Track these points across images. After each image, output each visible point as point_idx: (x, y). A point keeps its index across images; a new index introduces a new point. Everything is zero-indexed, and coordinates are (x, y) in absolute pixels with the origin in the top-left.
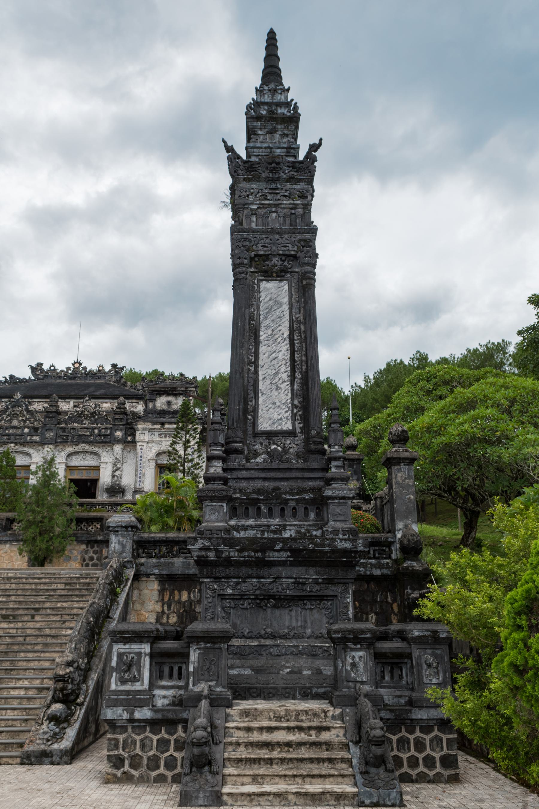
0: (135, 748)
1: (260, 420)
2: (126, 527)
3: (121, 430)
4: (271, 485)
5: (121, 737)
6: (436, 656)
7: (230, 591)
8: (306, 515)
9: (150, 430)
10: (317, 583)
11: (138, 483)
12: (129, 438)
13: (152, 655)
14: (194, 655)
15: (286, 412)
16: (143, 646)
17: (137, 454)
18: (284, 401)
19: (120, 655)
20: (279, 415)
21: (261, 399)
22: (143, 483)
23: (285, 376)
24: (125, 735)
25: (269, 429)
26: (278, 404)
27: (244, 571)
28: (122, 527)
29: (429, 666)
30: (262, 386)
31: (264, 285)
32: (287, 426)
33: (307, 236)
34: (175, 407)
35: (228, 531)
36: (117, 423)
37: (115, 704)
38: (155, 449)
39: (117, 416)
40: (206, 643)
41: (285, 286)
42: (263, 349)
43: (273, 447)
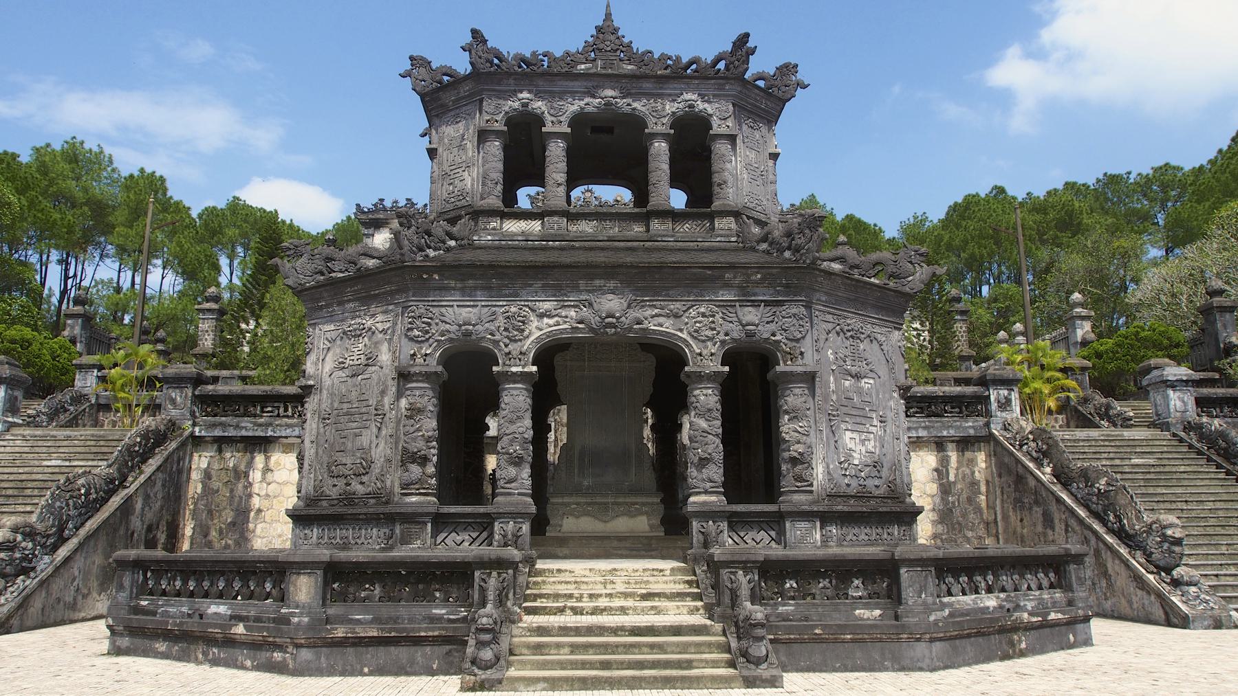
2: (1187, 382)
28: (1183, 381)
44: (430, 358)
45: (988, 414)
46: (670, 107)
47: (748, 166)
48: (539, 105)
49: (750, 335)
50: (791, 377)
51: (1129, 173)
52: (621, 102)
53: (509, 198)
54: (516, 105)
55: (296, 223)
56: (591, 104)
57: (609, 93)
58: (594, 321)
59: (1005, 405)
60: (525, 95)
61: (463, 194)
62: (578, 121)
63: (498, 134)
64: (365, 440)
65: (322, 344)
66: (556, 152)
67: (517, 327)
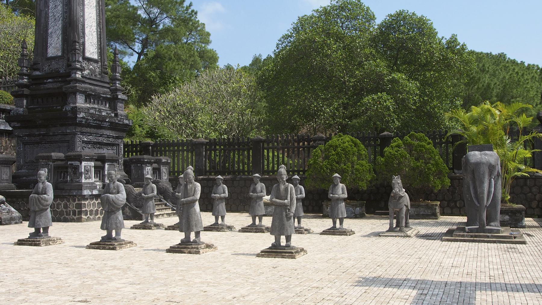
0: (91, 207)
1: (86, 51)
5: (86, 202)
6: (165, 168)
7: (86, 139)
8: (106, 105)
10: (113, 138)
13: (95, 167)
14: (107, 166)
15: (95, 49)
16: (91, 163)
18: (94, 43)
19: (85, 166)
20: (93, 50)
21: (86, 38)
24: (88, 202)
25: (89, 56)
26: (92, 44)
27: (93, 130)
29: (164, 172)
32: (95, 57)
35: (89, 109)
37: (87, 188)
40: (110, 162)
42: (86, 10)
43: (91, 67)
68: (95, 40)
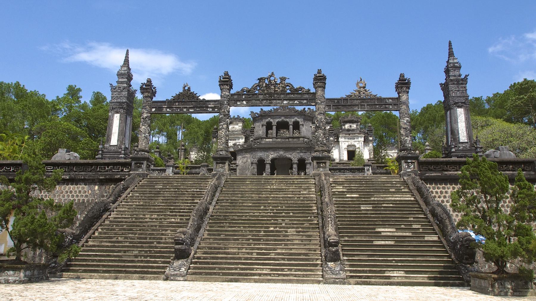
1: (460, 140)
3: (332, 137)
4: (464, 153)
9: (344, 137)
11: (341, 157)
12: (336, 140)
17: (340, 146)
21: (460, 135)
22: (343, 157)
23: (465, 130)
30: (460, 132)
31: (457, 109)
32: (466, 141)
33: (467, 98)
34: (353, 128)
36: (330, 134)
38: (347, 144)
39: (331, 132)
41: (462, 109)
44: (256, 161)
45: (365, 172)
46: (293, 120)
47: (306, 129)
48: (271, 120)
49: (302, 157)
50: (307, 163)
51: (482, 97)
52: (285, 119)
53: (267, 133)
54: (268, 120)
55: (197, 118)
56: (280, 120)
57: (283, 118)
58: (279, 155)
59: (368, 170)
60: (269, 119)
61: (259, 134)
62: (278, 123)
63: (265, 125)
64: (246, 173)
65: (239, 159)
66: (274, 127)
67: (268, 156)
68: (465, 134)
